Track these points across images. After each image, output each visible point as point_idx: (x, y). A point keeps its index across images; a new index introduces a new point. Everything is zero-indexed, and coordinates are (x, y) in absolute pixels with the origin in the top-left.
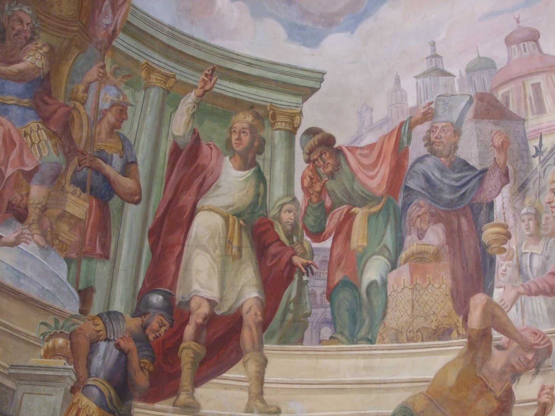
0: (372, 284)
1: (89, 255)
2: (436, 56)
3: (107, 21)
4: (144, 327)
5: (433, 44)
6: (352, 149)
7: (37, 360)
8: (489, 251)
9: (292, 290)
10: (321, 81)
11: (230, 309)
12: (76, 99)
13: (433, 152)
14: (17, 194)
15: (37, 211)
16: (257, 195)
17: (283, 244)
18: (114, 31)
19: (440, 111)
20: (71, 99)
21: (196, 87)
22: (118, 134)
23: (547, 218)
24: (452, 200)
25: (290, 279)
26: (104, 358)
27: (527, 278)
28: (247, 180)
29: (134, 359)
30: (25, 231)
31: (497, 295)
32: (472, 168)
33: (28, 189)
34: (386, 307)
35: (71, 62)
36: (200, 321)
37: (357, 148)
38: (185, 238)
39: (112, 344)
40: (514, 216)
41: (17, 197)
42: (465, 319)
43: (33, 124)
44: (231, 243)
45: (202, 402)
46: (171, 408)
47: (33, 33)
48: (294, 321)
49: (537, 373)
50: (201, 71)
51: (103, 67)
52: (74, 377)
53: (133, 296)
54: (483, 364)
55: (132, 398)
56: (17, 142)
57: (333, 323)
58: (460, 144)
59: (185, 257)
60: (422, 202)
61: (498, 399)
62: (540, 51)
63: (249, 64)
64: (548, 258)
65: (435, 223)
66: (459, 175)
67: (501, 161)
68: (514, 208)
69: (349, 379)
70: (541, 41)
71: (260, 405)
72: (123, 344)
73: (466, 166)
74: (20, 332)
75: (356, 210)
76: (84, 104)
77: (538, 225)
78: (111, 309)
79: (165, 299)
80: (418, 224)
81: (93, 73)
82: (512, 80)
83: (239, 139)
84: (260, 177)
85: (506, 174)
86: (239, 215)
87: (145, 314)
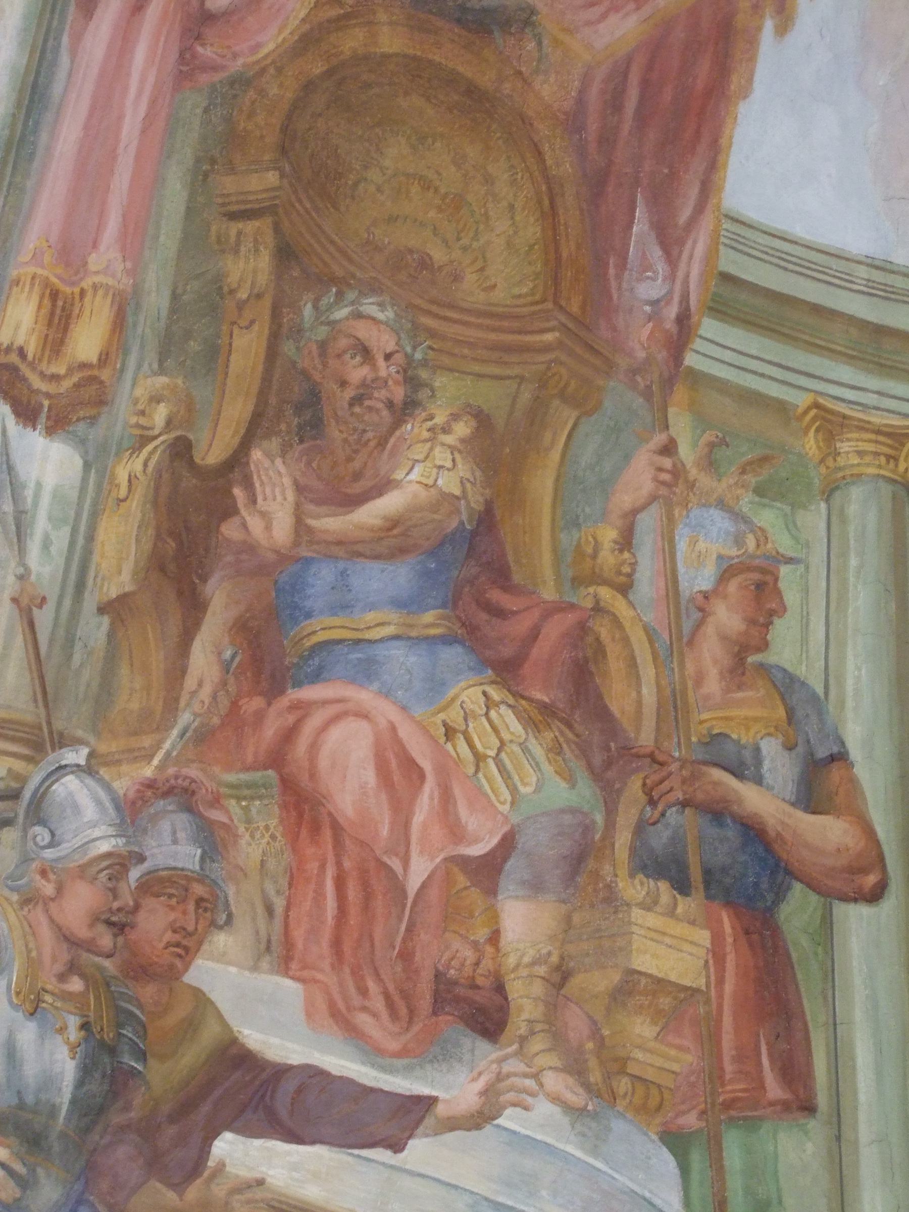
12: (596, 579)
14: (457, 944)
15: (538, 989)
18: (683, 319)
20: (578, 582)
22: (762, 668)
30: (514, 1066)
33: (494, 917)
35: (555, 456)
47: (412, 382)
51: (669, 449)
56: (426, 765)
76: (625, 589)
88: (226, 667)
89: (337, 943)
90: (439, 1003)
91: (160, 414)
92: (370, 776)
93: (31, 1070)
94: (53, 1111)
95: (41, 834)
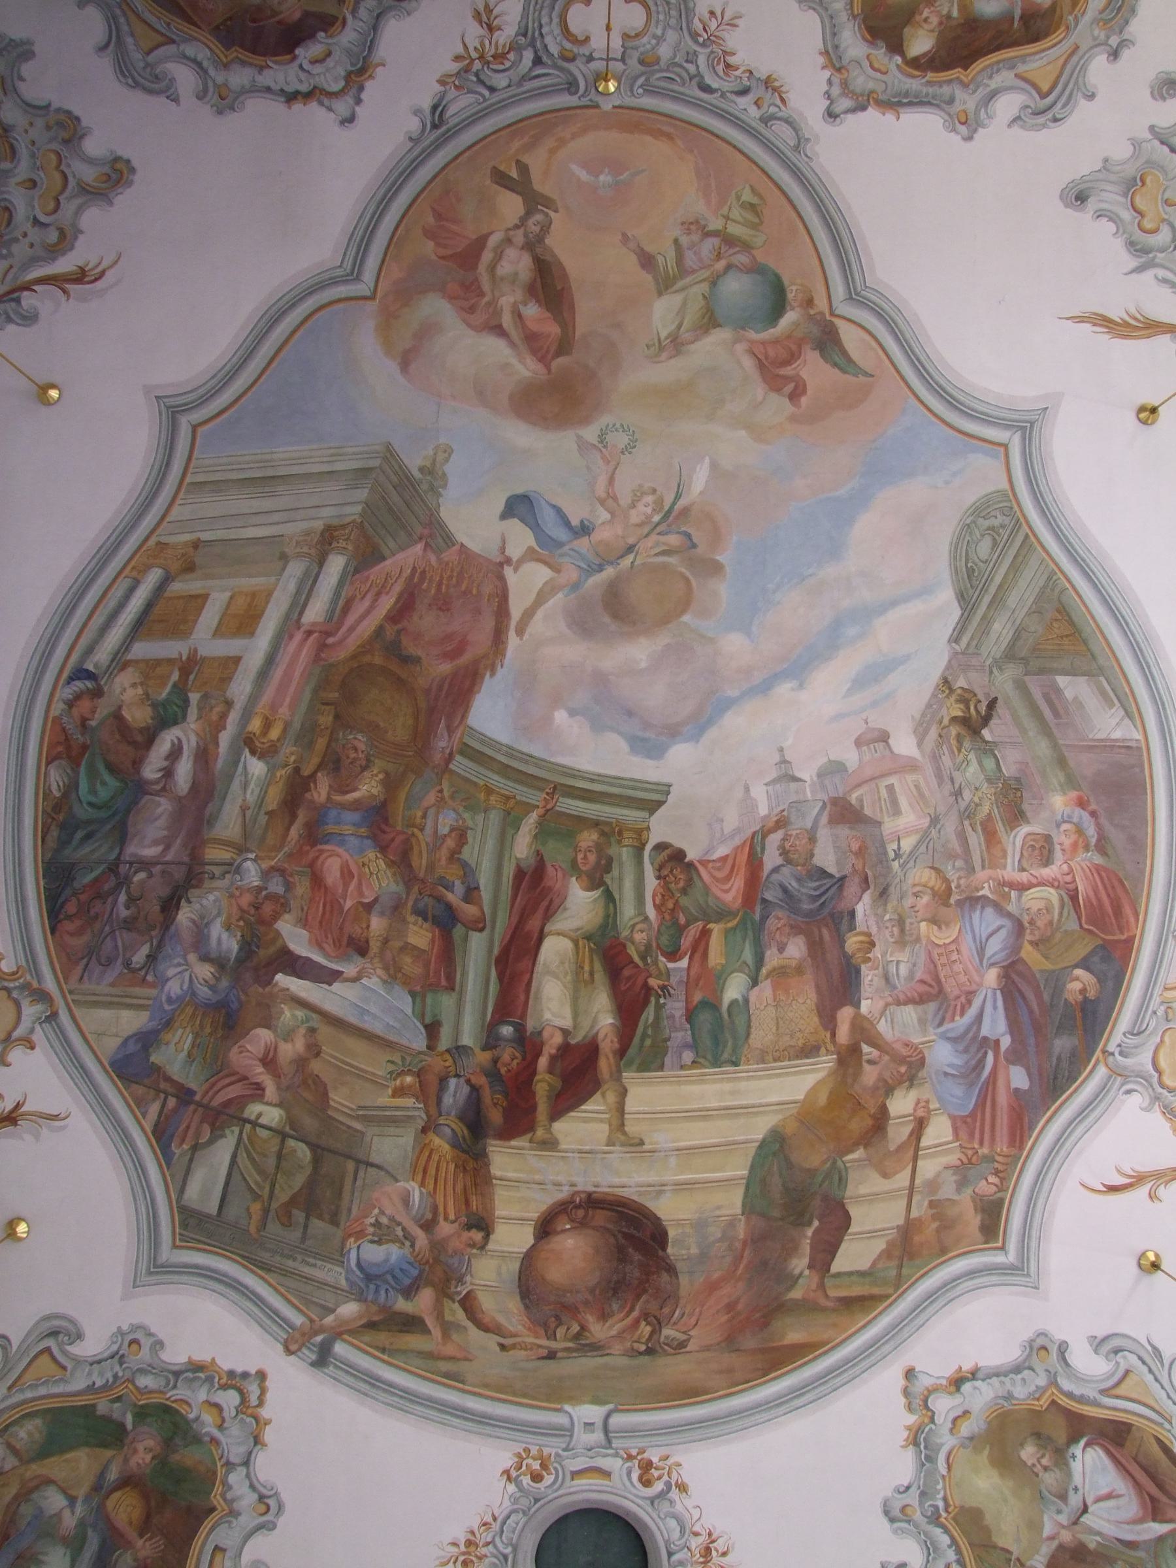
0: (734, 1003)
1: (434, 987)
2: (784, 761)
3: (442, 744)
4: (495, 1061)
5: (781, 750)
6: (705, 863)
7: (385, 1099)
8: (854, 961)
9: (649, 1014)
10: (668, 793)
11: (585, 1037)
12: (414, 826)
13: (789, 861)
14: (357, 927)
15: (379, 944)
16: (607, 916)
17: (637, 966)
18: (451, 755)
19: (793, 819)
20: (408, 826)
21: (538, 807)
23: (911, 924)
24: (811, 911)
25: (646, 1002)
26: (454, 1096)
27: (895, 987)
28: (595, 900)
29: (487, 1096)
31: (865, 1006)
32: (831, 876)
33: (369, 921)
34: (749, 1027)
35: (407, 789)
36: (553, 1051)
37: (709, 861)
38: (534, 965)
39: (462, 1080)
40: (877, 923)
41: (357, 930)
42: (833, 1035)
43: (371, 854)
44: (582, 968)
45: (560, 1137)
46: (527, 1144)
47: (368, 760)
48: (652, 1046)
49: (911, 1086)
50: (541, 790)
51: (441, 791)
52: (424, 1117)
53: (482, 1026)
54: (855, 1081)
55: (486, 1136)
57: (694, 1046)
58: (816, 851)
59: (534, 984)
60: (780, 914)
61: (873, 1117)
62: (892, 752)
63: (592, 780)
64: (914, 965)
65: (796, 935)
66: (817, 883)
67: (859, 867)
68: (876, 915)
69: (715, 1104)
70: (890, 741)
71: (623, 1138)
72: (474, 1081)
73: (823, 873)
74: (366, 1072)
75: (711, 926)
76: (422, 830)
77: (902, 931)
78: (460, 1044)
79: (516, 1030)
80: (777, 936)
81: (431, 798)
82: (866, 782)
83: (585, 858)
84: (609, 897)
85: (866, 880)
86: (588, 937)
87: (495, 1047)
88: (300, 836)
89: (321, 922)
90: (348, 945)
91: (293, 758)
92: (338, 874)
93: (224, 947)
94: (229, 960)
95: (238, 878)
